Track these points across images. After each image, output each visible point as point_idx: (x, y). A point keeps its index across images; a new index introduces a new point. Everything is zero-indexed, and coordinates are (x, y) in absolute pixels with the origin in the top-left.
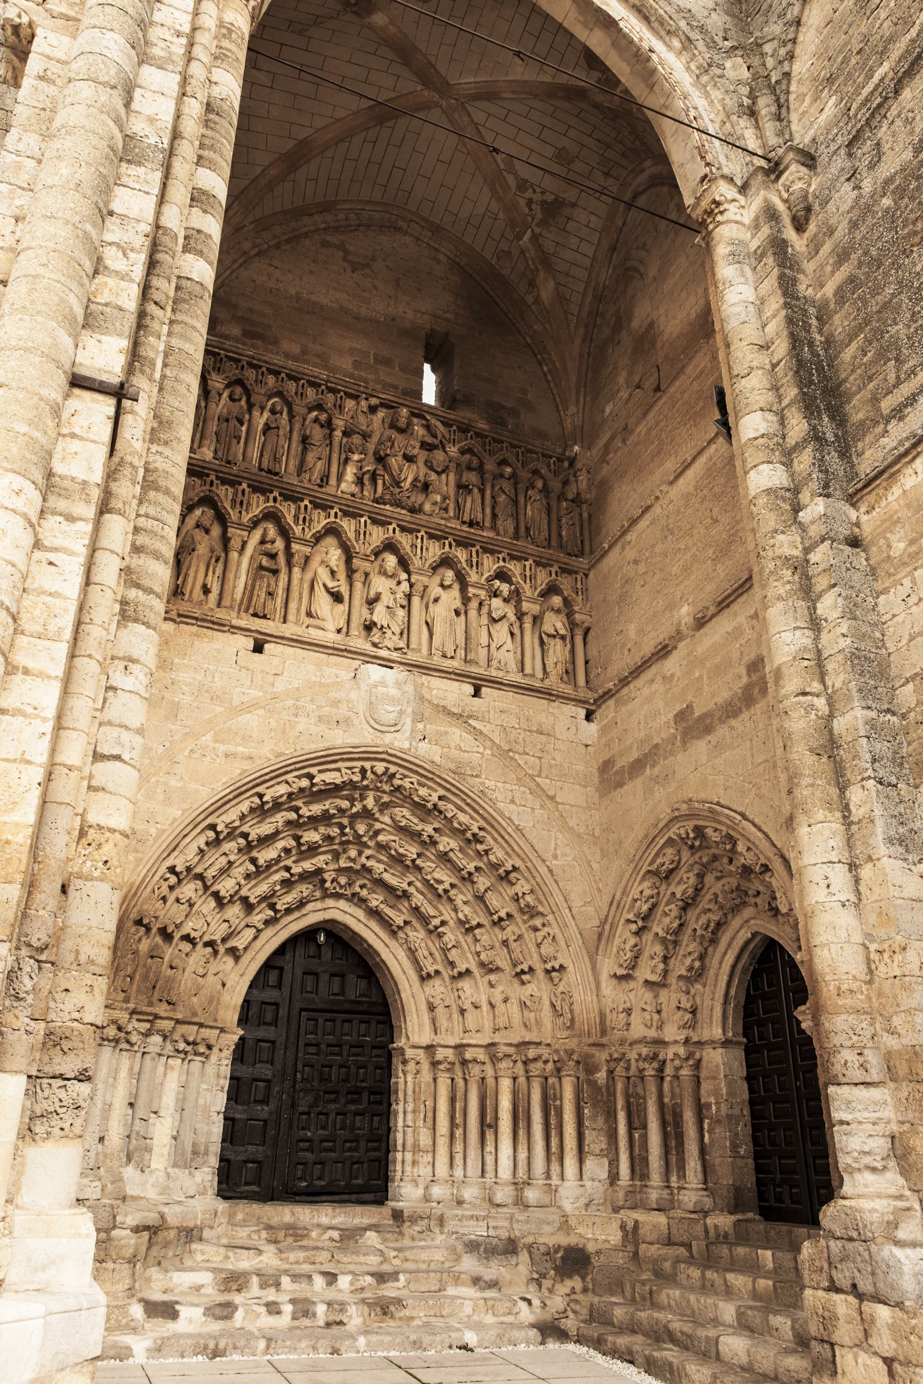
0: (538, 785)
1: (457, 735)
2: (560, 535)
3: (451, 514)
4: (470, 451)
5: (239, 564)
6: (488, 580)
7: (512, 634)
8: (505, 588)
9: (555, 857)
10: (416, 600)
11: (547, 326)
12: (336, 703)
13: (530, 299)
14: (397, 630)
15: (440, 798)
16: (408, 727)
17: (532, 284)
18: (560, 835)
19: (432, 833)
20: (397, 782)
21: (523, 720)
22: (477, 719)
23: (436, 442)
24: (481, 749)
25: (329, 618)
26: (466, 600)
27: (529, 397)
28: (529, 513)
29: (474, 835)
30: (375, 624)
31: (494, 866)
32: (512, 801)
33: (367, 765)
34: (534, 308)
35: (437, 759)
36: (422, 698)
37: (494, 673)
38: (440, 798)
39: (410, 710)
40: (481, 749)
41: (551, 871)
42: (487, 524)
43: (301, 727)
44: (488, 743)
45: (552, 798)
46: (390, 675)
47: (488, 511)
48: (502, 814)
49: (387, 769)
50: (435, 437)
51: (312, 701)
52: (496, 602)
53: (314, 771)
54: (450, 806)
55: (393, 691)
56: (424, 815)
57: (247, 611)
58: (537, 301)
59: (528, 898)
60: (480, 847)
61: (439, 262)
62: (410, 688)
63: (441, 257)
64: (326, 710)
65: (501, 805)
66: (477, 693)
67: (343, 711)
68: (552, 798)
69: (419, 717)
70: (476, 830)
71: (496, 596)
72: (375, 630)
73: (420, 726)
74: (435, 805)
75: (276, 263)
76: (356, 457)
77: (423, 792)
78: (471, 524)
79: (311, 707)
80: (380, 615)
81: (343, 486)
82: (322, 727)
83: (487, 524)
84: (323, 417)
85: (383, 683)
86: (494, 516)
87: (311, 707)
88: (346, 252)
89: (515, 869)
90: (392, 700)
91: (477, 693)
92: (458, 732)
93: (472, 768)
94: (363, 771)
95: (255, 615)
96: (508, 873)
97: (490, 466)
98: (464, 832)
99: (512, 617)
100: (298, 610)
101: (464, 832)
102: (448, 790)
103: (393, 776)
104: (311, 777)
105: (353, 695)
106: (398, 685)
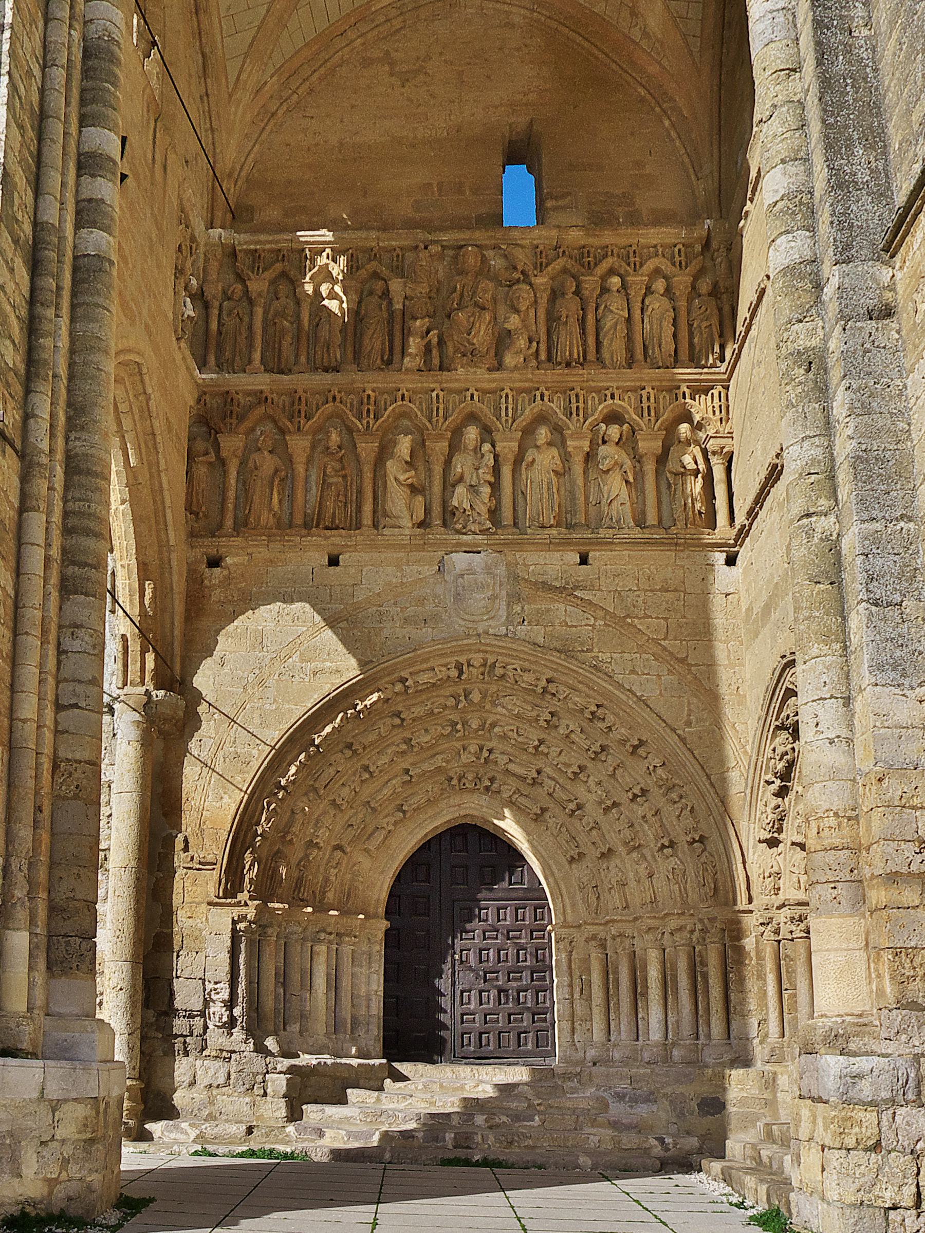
0: (665, 649)
1: (561, 609)
2: (691, 344)
3: (543, 357)
4: (565, 271)
5: (307, 478)
6: (594, 428)
7: (627, 482)
8: (614, 431)
9: (689, 724)
10: (506, 471)
11: (665, 63)
12: (421, 601)
13: (636, 34)
14: (483, 510)
15: (549, 681)
16: (503, 613)
17: (634, 14)
18: (695, 700)
19: (549, 717)
20: (499, 671)
21: (643, 580)
22: (585, 588)
23: (516, 275)
24: (592, 622)
25: (406, 514)
26: (566, 458)
27: (648, 170)
28: (647, 326)
29: (592, 713)
30: (456, 508)
31: (623, 742)
32: (633, 672)
33: (463, 659)
34: (644, 44)
35: (541, 640)
36: (516, 578)
37: (602, 533)
38: (549, 681)
39: (504, 593)
40: (592, 622)
41: (683, 740)
42: (591, 356)
43: (386, 633)
44: (601, 613)
45: (682, 661)
46: (477, 560)
47: (591, 340)
48: (620, 686)
49: (485, 660)
50: (515, 268)
51: (395, 603)
52: (603, 450)
53: (405, 674)
54: (561, 688)
55: (480, 578)
56: (538, 702)
57: (317, 526)
58: (645, 34)
59: (659, 771)
60: (600, 725)
61: (513, 26)
62: (501, 571)
63: (517, 19)
64: (411, 610)
65: (619, 678)
66: (584, 561)
67: (429, 607)
68: (682, 661)
69: (515, 597)
70: (594, 708)
71: (604, 442)
72: (457, 513)
73: (518, 608)
74: (545, 689)
75: (311, 112)
76: (418, 323)
77: (528, 678)
78: (568, 365)
79: (394, 610)
80: (460, 497)
81: (406, 360)
82: (409, 628)
83: (591, 356)
84: (379, 286)
85: (471, 571)
86: (598, 344)
87: (394, 610)
88: (392, 64)
89: (642, 743)
90: (482, 587)
91: (584, 561)
92: (562, 607)
93: (582, 644)
94: (459, 668)
95: (327, 528)
96: (635, 748)
97: (590, 283)
98: (581, 711)
99: (628, 464)
100: (375, 512)
101: (581, 711)
102: (556, 670)
103: (494, 665)
104: (403, 680)
105: (439, 590)
106: (488, 570)
